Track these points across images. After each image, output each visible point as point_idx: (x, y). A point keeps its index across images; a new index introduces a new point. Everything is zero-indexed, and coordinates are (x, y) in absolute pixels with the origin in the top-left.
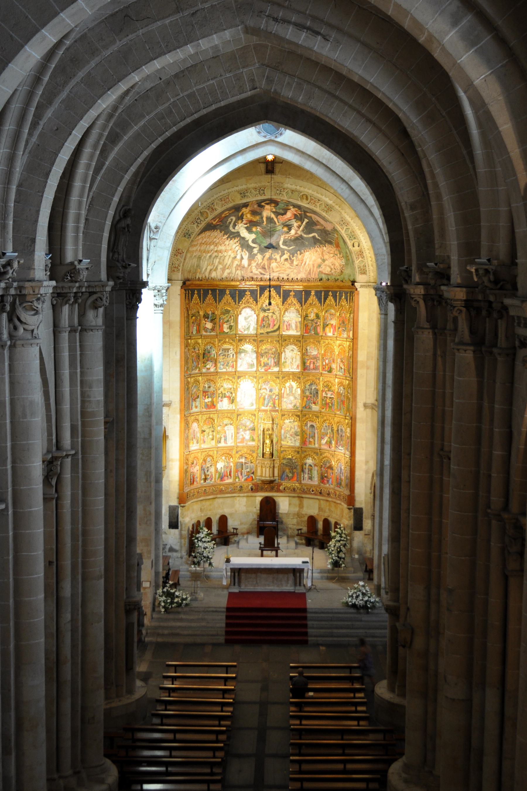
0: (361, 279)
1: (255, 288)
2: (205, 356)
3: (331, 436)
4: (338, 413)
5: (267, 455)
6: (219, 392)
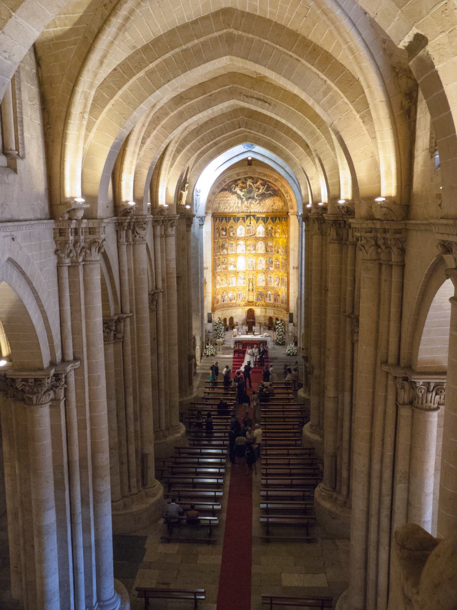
0: (291, 211)
1: (244, 216)
2: (223, 247)
4: (282, 271)
5: (251, 290)
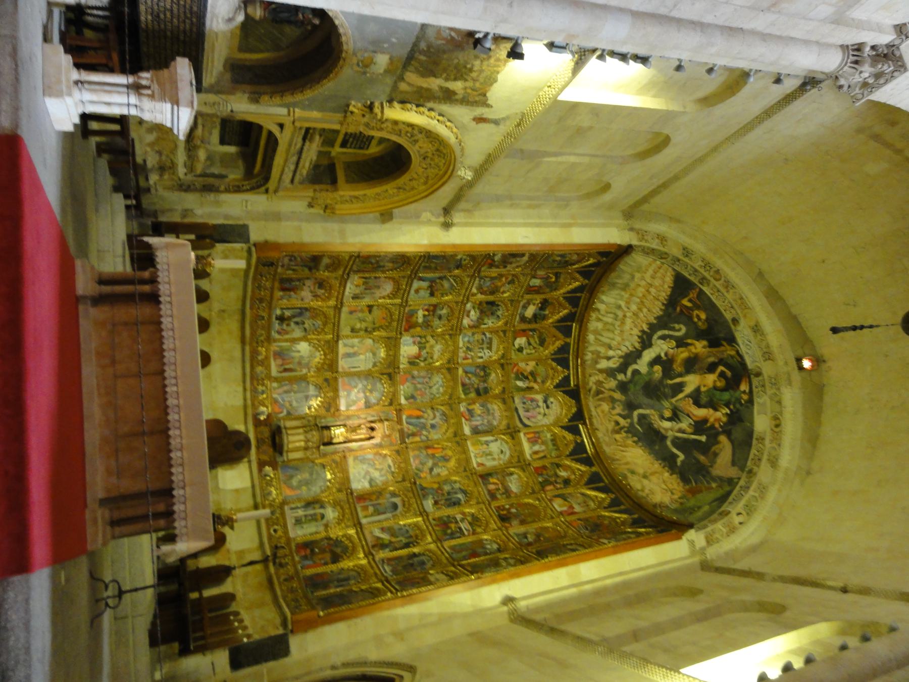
2: (489, 308)
3: (397, 545)
6: (429, 338)
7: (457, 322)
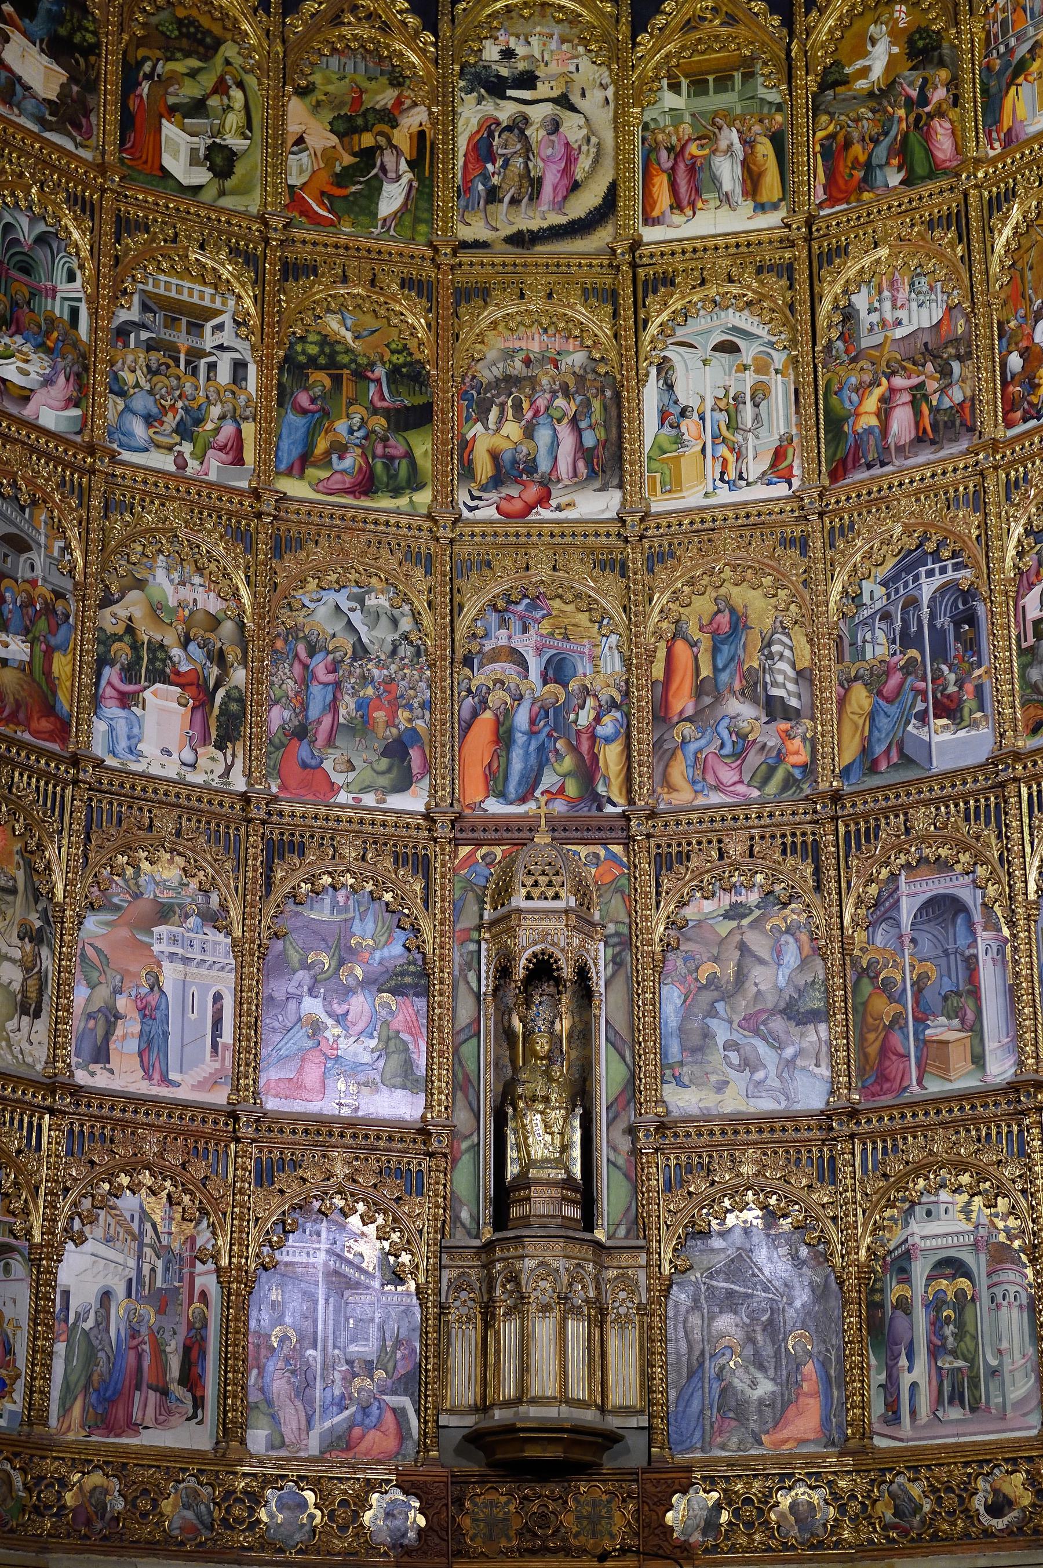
6: (110, 620)
7: (49, 457)
